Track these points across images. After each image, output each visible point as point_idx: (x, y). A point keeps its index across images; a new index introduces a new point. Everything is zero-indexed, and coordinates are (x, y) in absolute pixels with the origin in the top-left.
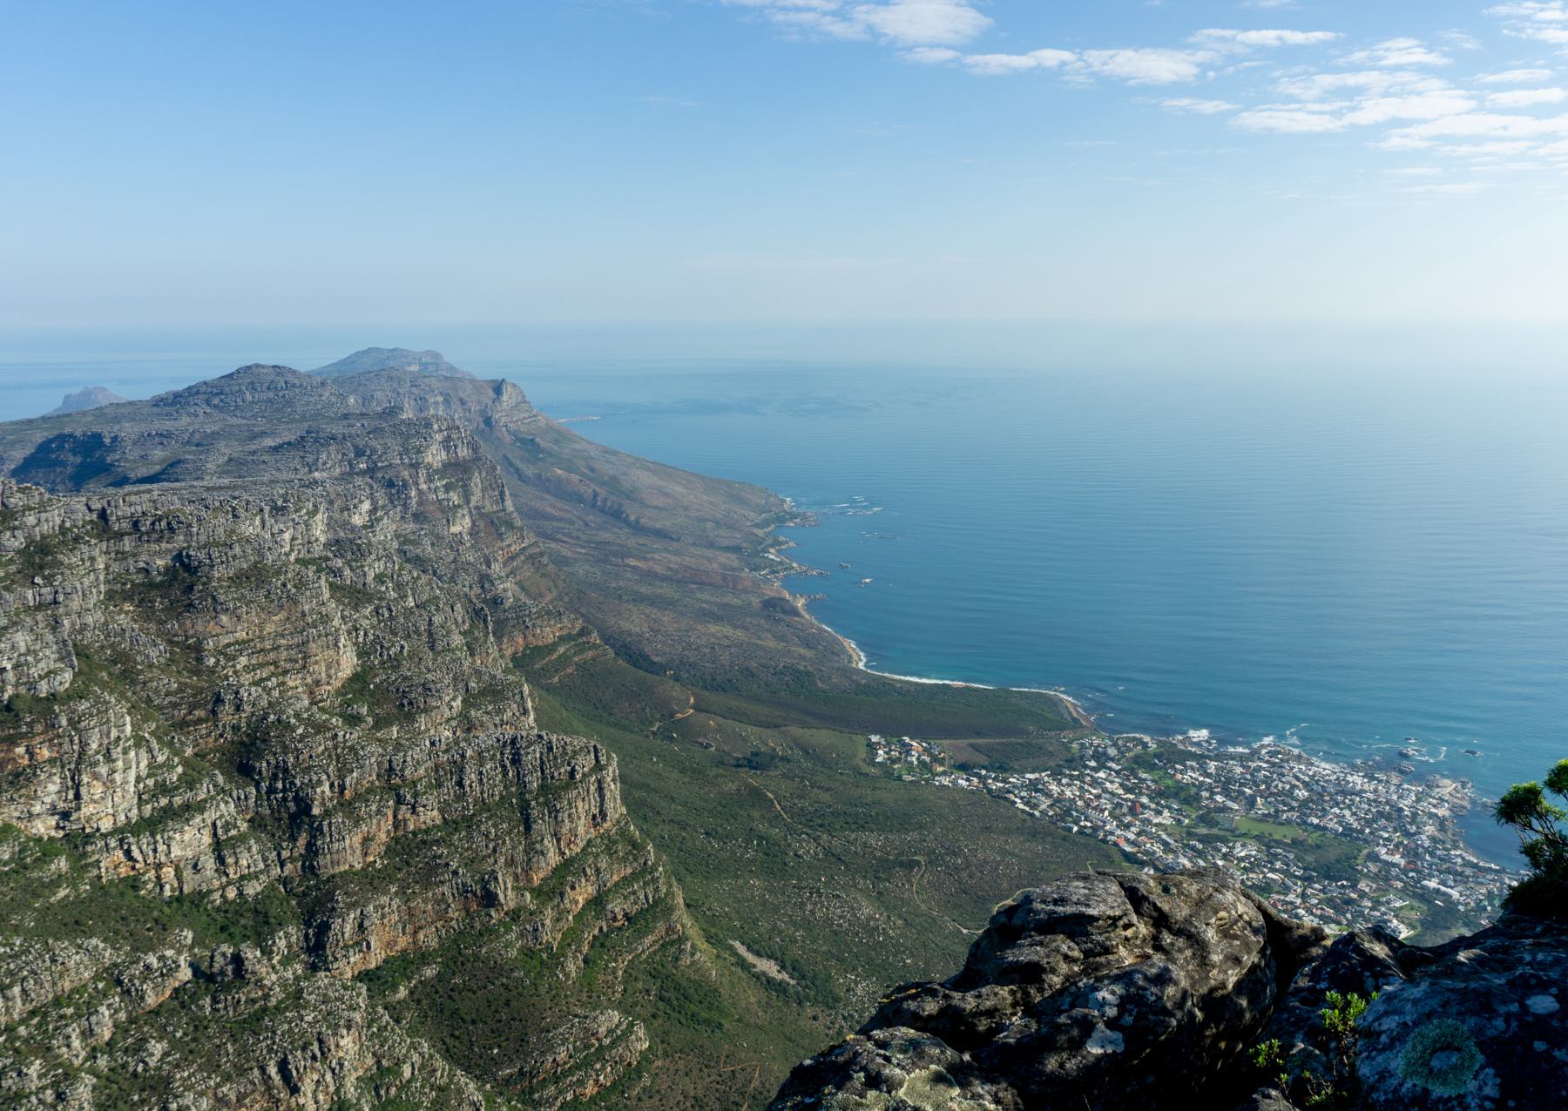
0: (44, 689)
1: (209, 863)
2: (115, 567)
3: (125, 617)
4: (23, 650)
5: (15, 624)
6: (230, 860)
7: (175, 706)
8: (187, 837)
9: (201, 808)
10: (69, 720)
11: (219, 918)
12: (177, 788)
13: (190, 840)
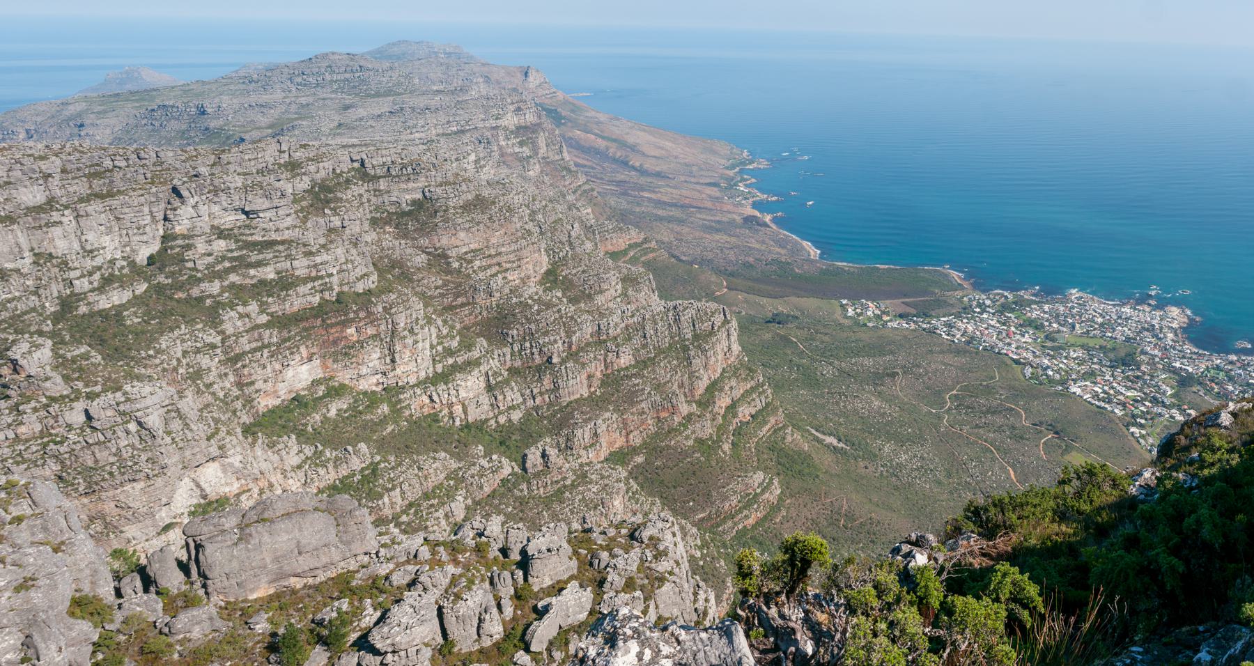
0: (360, 288)
1: (485, 400)
2: (374, 200)
3: (389, 239)
4: (343, 260)
5: (331, 242)
6: (500, 397)
7: (442, 295)
8: (469, 384)
9: (477, 363)
10: (384, 308)
11: (496, 435)
12: (459, 351)
13: (471, 386)
